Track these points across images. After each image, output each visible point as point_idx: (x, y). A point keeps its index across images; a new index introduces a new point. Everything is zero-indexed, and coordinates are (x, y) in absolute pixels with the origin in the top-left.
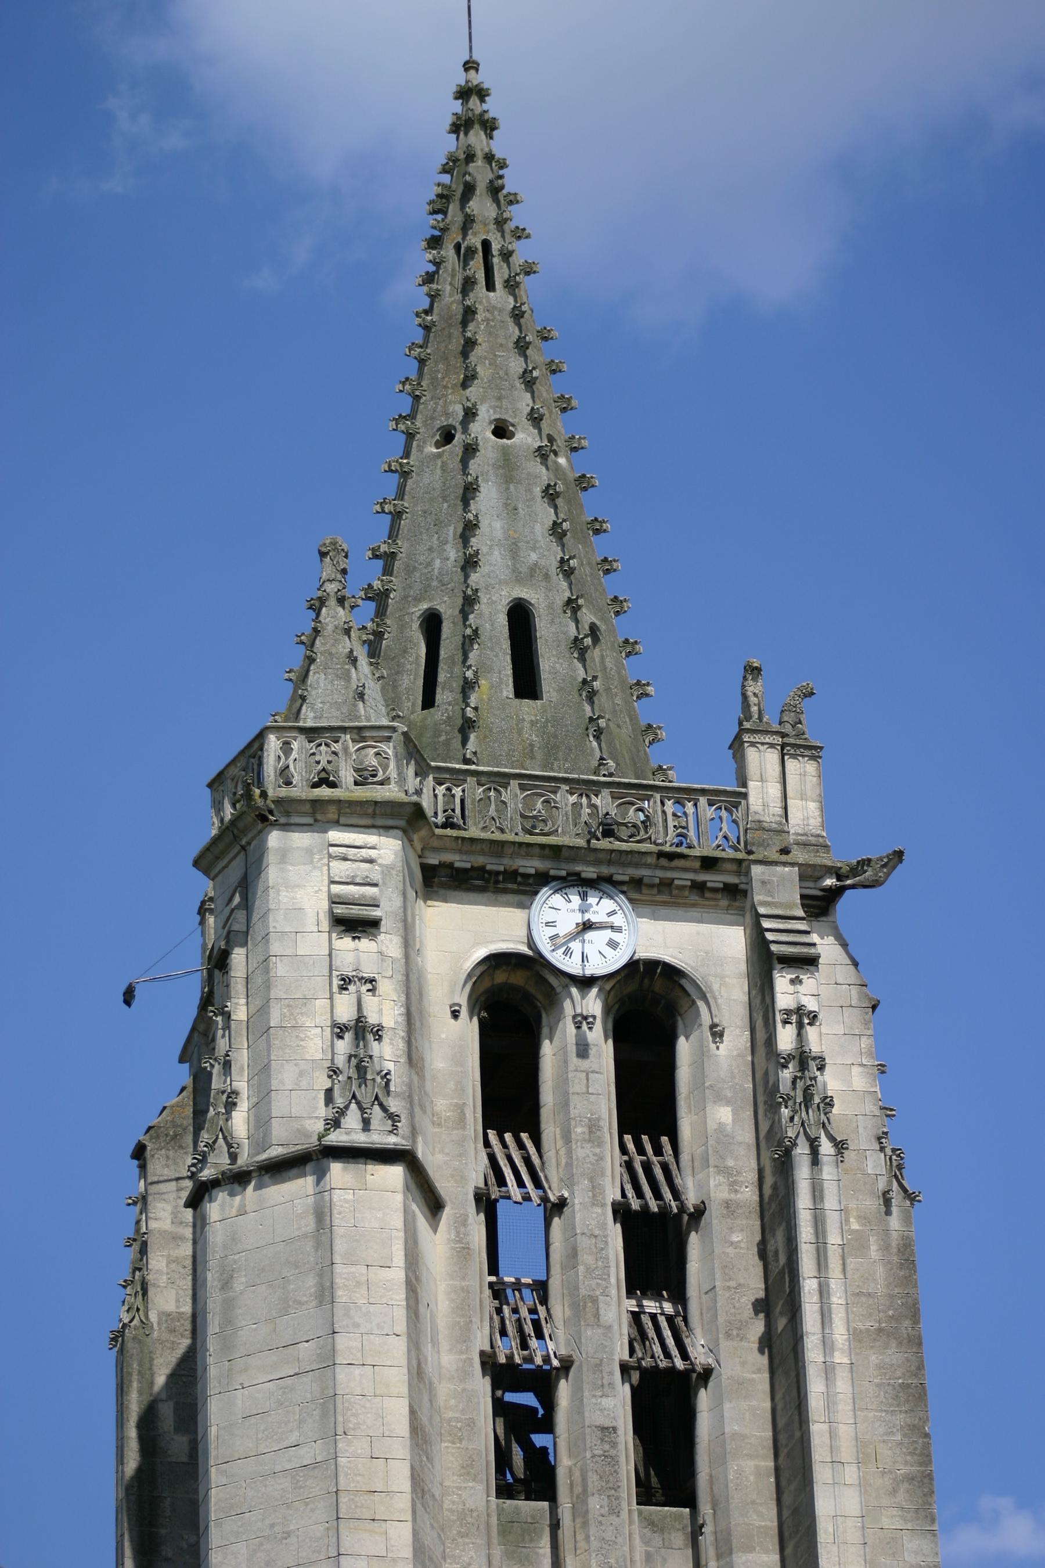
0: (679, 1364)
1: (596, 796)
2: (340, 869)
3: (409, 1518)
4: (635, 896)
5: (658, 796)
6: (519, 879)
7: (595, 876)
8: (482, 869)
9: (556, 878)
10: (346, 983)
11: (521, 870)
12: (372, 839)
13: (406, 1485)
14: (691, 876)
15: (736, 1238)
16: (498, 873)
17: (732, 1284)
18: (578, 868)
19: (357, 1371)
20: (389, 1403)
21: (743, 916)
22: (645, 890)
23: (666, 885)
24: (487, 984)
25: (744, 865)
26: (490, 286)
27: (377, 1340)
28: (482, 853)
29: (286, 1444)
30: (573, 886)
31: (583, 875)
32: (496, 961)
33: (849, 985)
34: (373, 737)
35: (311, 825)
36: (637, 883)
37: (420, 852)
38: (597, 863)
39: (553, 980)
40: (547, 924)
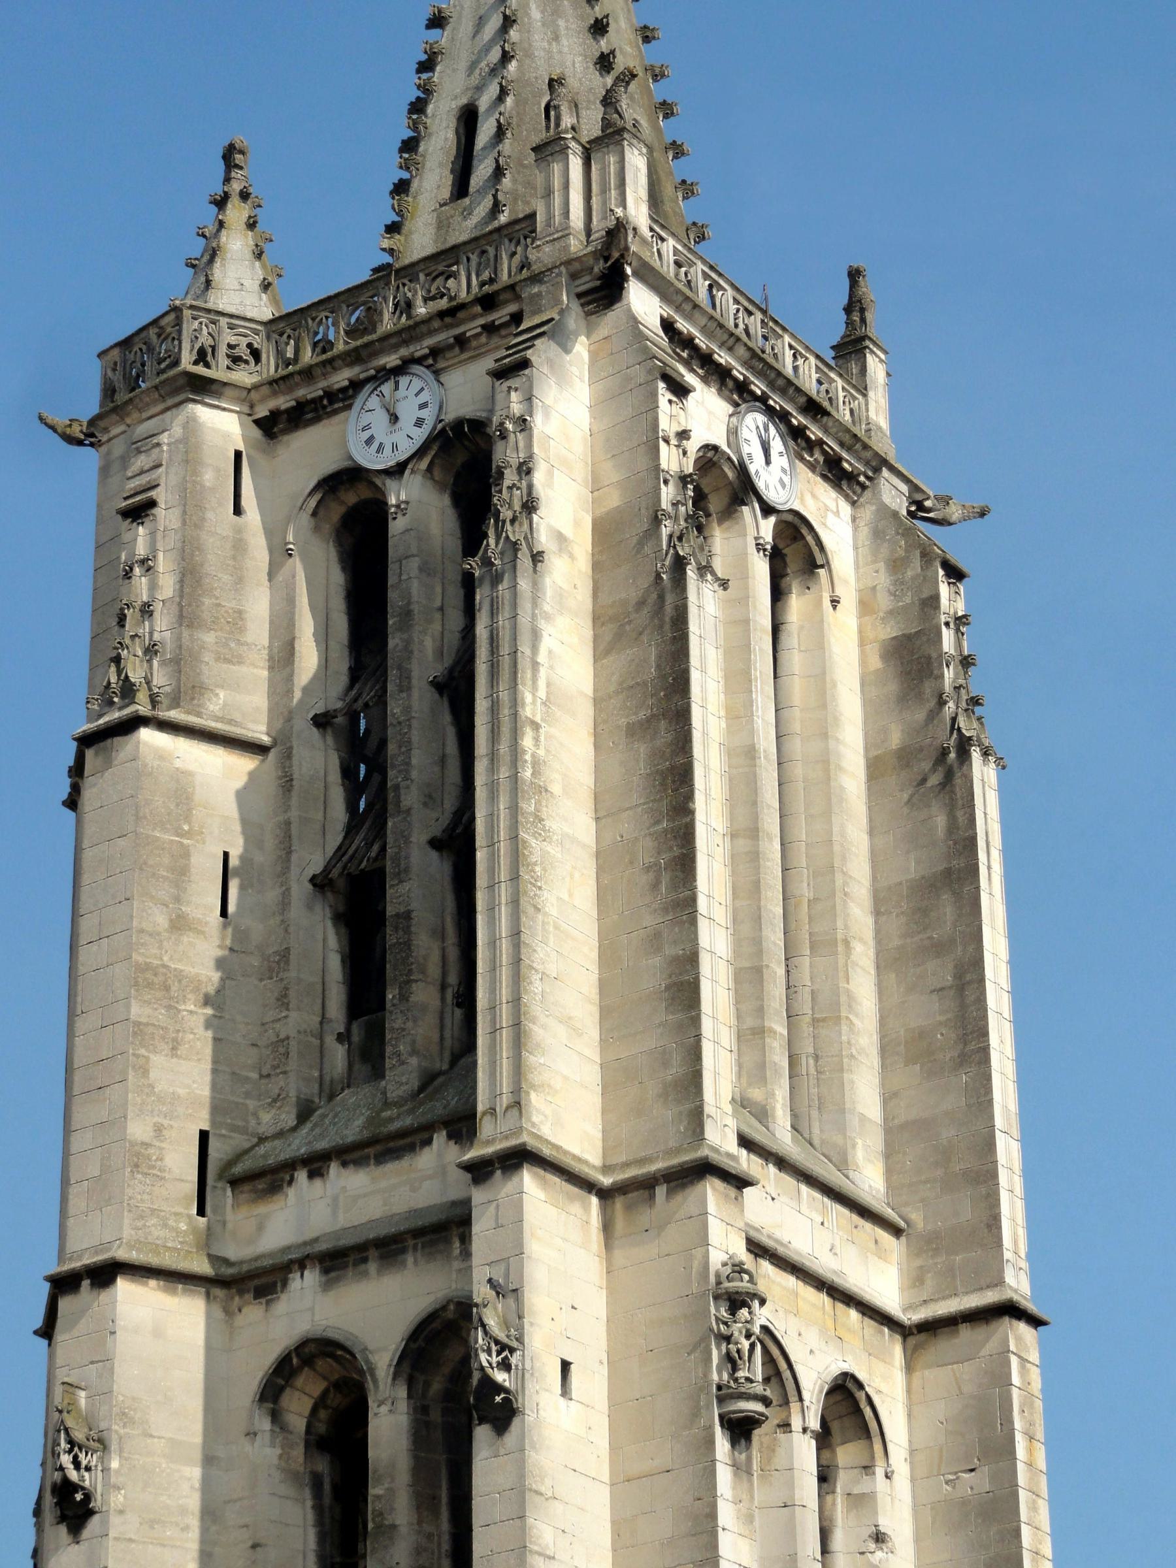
7: (399, 362)
14: (482, 321)
16: (321, 398)
24: (336, 512)
38: (396, 347)
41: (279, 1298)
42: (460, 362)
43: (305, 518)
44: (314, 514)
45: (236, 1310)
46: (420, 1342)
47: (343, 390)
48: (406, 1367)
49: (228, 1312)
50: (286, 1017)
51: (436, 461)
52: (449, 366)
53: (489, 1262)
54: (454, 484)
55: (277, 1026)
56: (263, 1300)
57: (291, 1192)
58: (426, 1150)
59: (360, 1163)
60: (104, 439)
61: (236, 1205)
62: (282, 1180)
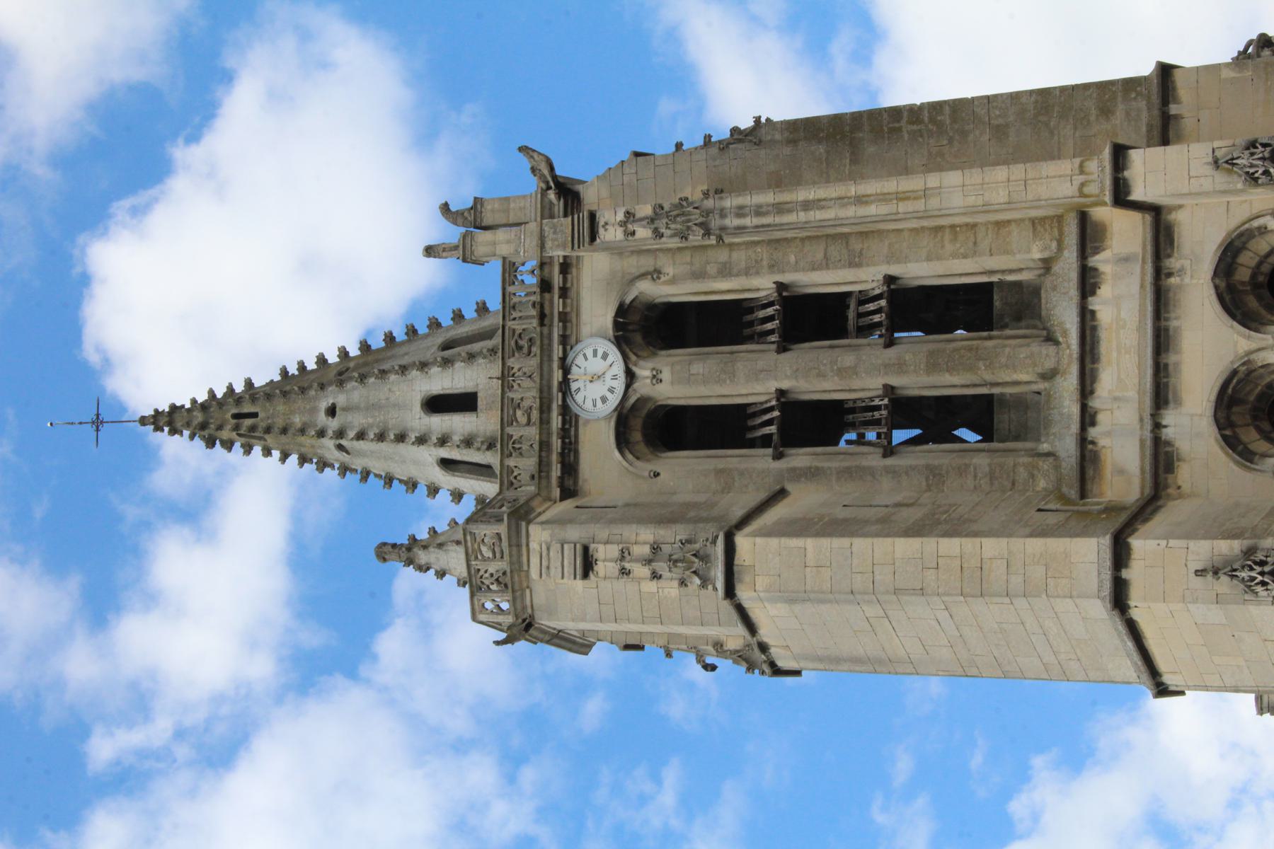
0: (883, 303)
1: (513, 368)
2: (555, 570)
3: (977, 540)
4: (573, 340)
5: (509, 324)
6: (567, 426)
7: (560, 371)
8: (562, 455)
10: (625, 572)
11: (560, 426)
12: (534, 545)
13: (956, 541)
15: (792, 258)
16: (563, 442)
17: (824, 263)
18: (555, 384)
19: (877, 578)
21: (583, 256)
22: (568, 333)
23: (564, 318)
24: (642, 448)
25: (545, 261)
26: (255, 415)
27: (855, 561)
29: (938, 627)
30: (569, 386)
31: (560, 380)
32: (622, 441)
33: (623, 174)
34: (472, 545)
35: (531, 591)
36: (564, 340)
37: (552, 502)
39: (632, 400)
40: (595, 406)
41: (1177, 449)
42: (577, 325)
43: (638, 463)
44: (638, 458)
45: (1179, 491)
46: (1238, 313)
48: (1254, 325)
49: (1180, 496)
50: (975, 469)
51: (635, 351)
52: (577, 335)
53: (1188, 177)
54: (654, 347)
55: (980, 475)
56: (1176, 464)
57: (1102, 442)
58: (1100, 315)
59: (1094, 378)
60: (529, 611)
61: (1101, 495)
62: (1091, 451)
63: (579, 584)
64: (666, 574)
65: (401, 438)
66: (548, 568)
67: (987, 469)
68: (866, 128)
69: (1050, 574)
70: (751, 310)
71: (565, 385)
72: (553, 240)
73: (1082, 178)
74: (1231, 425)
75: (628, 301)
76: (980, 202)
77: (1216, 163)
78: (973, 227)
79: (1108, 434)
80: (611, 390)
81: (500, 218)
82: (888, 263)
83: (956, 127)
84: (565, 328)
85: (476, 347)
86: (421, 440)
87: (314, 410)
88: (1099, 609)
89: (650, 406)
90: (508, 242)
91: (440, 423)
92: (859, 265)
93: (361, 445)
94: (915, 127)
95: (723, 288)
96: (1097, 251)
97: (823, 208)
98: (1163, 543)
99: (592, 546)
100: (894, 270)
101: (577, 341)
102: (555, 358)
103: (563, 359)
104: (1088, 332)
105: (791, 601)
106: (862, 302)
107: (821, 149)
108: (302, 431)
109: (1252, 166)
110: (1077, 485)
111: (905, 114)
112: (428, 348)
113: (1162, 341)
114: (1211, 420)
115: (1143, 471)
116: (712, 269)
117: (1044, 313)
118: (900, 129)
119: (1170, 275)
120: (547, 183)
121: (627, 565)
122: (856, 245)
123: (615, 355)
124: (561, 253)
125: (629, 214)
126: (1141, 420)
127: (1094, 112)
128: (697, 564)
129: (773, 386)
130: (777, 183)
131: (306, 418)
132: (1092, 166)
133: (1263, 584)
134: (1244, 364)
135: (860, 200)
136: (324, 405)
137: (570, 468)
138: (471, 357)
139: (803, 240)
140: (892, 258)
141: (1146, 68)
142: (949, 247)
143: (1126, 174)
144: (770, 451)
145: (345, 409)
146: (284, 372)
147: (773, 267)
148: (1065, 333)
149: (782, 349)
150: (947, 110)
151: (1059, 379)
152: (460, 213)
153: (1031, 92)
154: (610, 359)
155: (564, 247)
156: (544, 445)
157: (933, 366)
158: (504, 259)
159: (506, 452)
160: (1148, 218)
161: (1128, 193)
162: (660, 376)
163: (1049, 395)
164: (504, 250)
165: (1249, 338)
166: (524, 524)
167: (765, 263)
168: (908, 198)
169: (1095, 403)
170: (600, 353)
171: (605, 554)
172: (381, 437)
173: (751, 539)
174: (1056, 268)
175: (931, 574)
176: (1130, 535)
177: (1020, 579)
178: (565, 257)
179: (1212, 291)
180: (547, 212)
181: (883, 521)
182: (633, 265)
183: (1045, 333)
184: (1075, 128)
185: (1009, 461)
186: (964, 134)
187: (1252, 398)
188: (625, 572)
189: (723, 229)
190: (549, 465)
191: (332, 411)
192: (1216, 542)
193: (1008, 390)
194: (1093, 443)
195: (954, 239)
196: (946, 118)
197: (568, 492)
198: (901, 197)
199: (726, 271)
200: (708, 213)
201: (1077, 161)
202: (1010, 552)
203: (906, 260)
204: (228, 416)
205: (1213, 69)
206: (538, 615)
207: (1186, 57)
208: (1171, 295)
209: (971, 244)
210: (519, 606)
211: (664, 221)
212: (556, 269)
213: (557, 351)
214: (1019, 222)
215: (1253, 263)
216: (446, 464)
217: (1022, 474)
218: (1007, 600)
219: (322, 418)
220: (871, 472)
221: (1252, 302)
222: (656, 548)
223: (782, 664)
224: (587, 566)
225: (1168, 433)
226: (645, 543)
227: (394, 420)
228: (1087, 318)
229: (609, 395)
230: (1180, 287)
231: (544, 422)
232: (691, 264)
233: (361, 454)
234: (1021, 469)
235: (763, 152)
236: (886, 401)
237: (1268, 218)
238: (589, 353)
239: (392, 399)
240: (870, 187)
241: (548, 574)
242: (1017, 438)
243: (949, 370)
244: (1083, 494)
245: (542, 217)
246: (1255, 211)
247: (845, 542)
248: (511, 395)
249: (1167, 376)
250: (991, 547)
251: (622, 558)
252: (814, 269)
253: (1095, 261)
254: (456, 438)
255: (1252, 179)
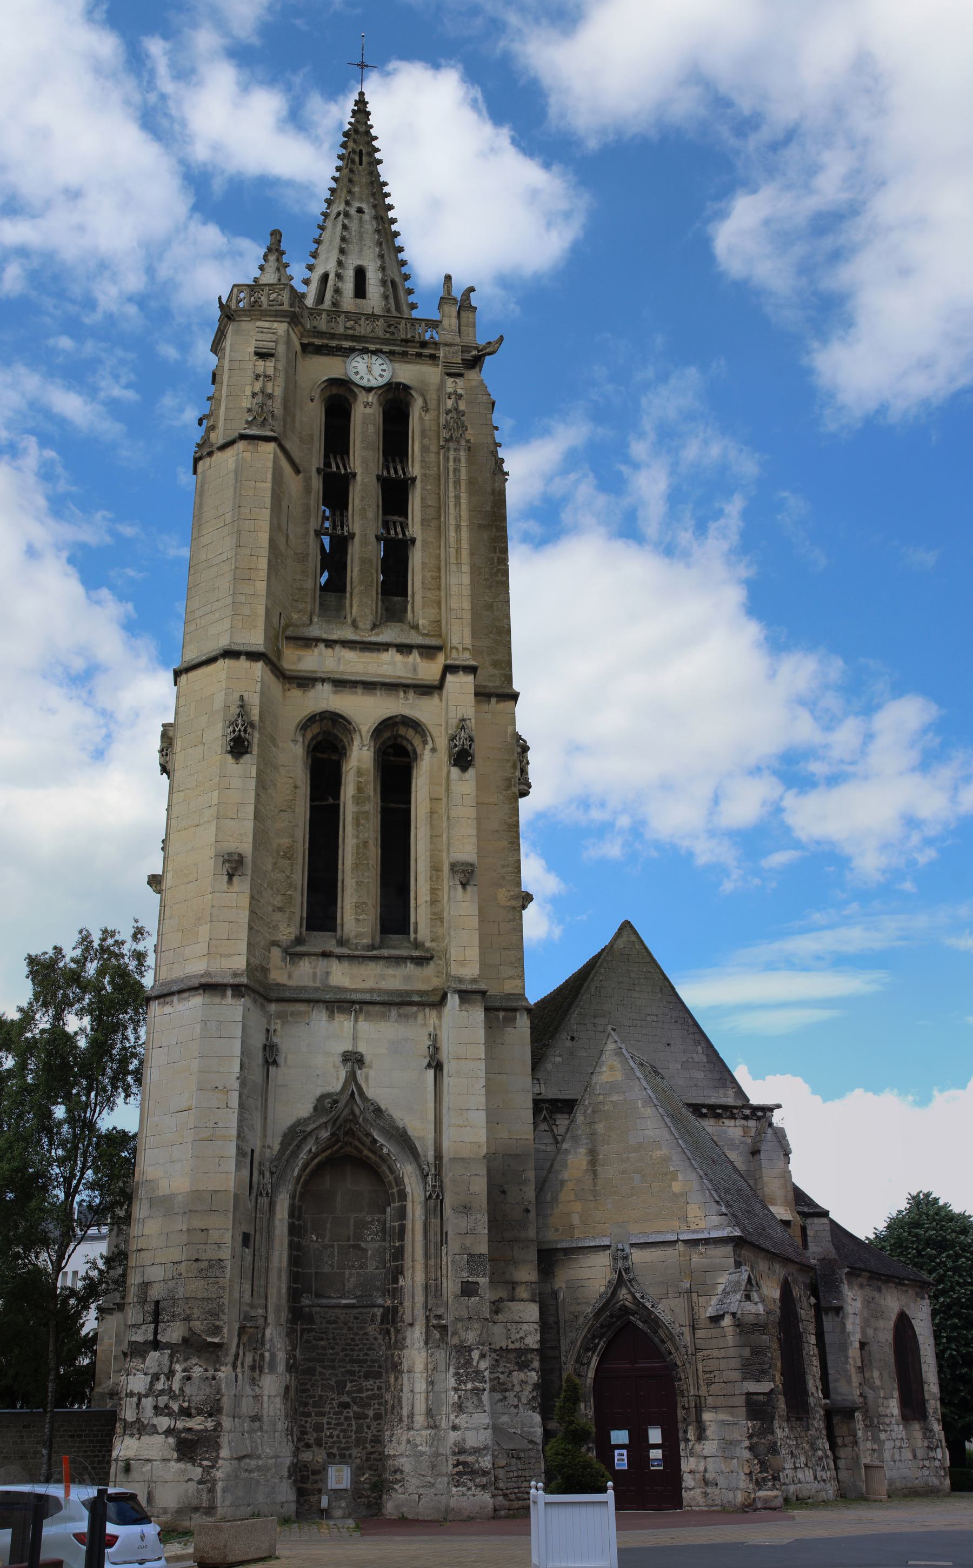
0: (401, 536)
2: (260, 336)
4: (392, 358)
5: (403, 321)
8: (327, 346)
9: (358, 350)
12: (275, 325)
13: (266, 567)
14: (417, 350)
16: (333, 347)
18: (367, 346)
19: (247, 522)
20: (259, 534)
23: (405, 354)
24: (328, 393)
26: (361, 164)
27: (257, 510)
28: (326, 338)
32: (332, 382)
36: (392, 353)
39: (356, 390)
43: (319, 390)
44: (322, 390)
47: (345, 349)
49: (284, 690)
57: (316, 650)
59: (352, 648)
60: (238, 319)
63: (252, 350)
64: (255, 401)
65: (342, 251)
66: (262, 332)
67: (305, 587)
68: (498, 534)
69: (245, 617)
70: (401, 462)
71: (365, 351)
72: (449, 351)
73: (461, 649)
74: (321, 720)
75: (411, 392)
76: (452, 593)
77: (464, 720)
78: (440, 590)
79: (321, 654)
80: (362, 378)
81: (464, 321)
82: (422, 541)
83: (494, 583)
84: (399, 354)
85: (392, 301)
86: (340, 263)
87: (361, 200)
88: (224, 642)
89: (351, 400)
90: (450, 325)
91: (349, 275)
92: (422, 524)
93: (339, 227)
94: (496, 561)
95: (415, 447)
96: (421, 654)
97: (456, 506)
98: (259, 679)
99: (273, 359)
100: (418, 543)
101: (391, 361)
102: (382, 347)
103: (381, 351)
104: (376, 647)
105: (236, 472)
106: (401, 524)
107: (488, 508)
108: (350, 192)
109: (460, 739)
110: (293, 635)
111: (503, 556)
112: (393, 272)
113: (369, 686)
114: (325, 709)
115: (299, 671)
116: (426, 441)
117: (389, 624)
118: (495, 552)
119: (405, 692)
120: (482, 351)
121: (261, 379)
122: (434, 524)
123: (382, 381)
124: (441, 355)
125: (461, 396)
126: (327, 672)
127: (496, 658)
128: (260, 419)
129: (358, 471)
130: (471, 482)
131: (357, 195)
132: (467, 655)
133: (234, 731)
134: (354, 728)
135: (458, 528)
136: (364, 206)
137: (320, 350)
138: (386, 297)
139: (439, 494)
140: (425, 543)
141: (516, 686)
142: (428, 574)
143: (461, 672)
144: (322, 466)
145: (361, 220)
146: (385, 184)
147: (425, 476)
148: (377, 634)
149: (379, 478)
150: (504, 579)
151: (352, 629)
152: (469, 298)
153: (509, 625)
154: (379, 379)
155: (445, 357)
156: (333, 336)
157: (363, 561)
158: (441, 322)
159: (330, 313)
160: (436, 683)
161: (451, 673)
162: (368, 407)
163: (343, 623)
164: (446, 322)
165: (368, 732)
166: (288, 320)
167: (427, 472)
168: (457, 554)
169: (338, 648)
170: (383, 373)
171: (268, 366)
172: (343, 239)
173: (272, 451)
174: (413, 632)
175: (248, 551)
176: (264, 661)
177: (243, 601)
178: (439, 357)
179: (394, 714)
180: (466, 349)
181: (279, 527)
182: (432, 396)
183: (378, 623)
184: (487, 647)
185: (309, 600)
186: (490, 587)
187: (335, 731)
188: (257, 377)
189: (448, 450)
190: (322, 338)
191: (360, 211)
192: (258, 708)
193: (348, 602)
194: (316, 646)
195: (432, 578)
196: (500, 578)
197: (304, 347)
198: (458, 550)
199: (425, 449)
200: (458, 442)
201: (470, 647)
202: (258, 596)
203: (423, 550)
204: (361, 147)
205: (513, 722)
206: (236, 324)
207: (522, 710)
208: (394, 692)
209: (429, 587)
210: (239, 313)
211: (455, 416)
212: (432, 352)
213: (386, 348)
214: (440, 613)
215: (408, 736)
216: (325, 277)
217: (301, 606)
218: (231, 593)
219: (356, 204)
220: (307, 522)
221: (387, 734)
222: (270, 396)
223: (201, 463)
224: (262, 355)
225: (319, 686)
226: (273, 390)
227: (353, 248)
228: (385, 647)
229: (359, 376)
230: (398, 697)
231: (346, 337)
232: (430, 430)
233: (334, 226)
234: (304, 605)
235: (489, 475)
236: (346, 534)
237: (432, 746)
238: (384, 367)
239: (365, 248)
240: (465, 534)
241: (258, 332)
242: (321, 604)
243: (361, 570)
244: (287, 638)
245: (462, 346)
246: (436, 739)
247: (268, 505)
248: (363, 319)
249: (350, 687)
250: (262, 586)
251: (266, 376)
252: (422, 499)
253: (415, 653)
254: (340, 284)
255: (453, 738)
